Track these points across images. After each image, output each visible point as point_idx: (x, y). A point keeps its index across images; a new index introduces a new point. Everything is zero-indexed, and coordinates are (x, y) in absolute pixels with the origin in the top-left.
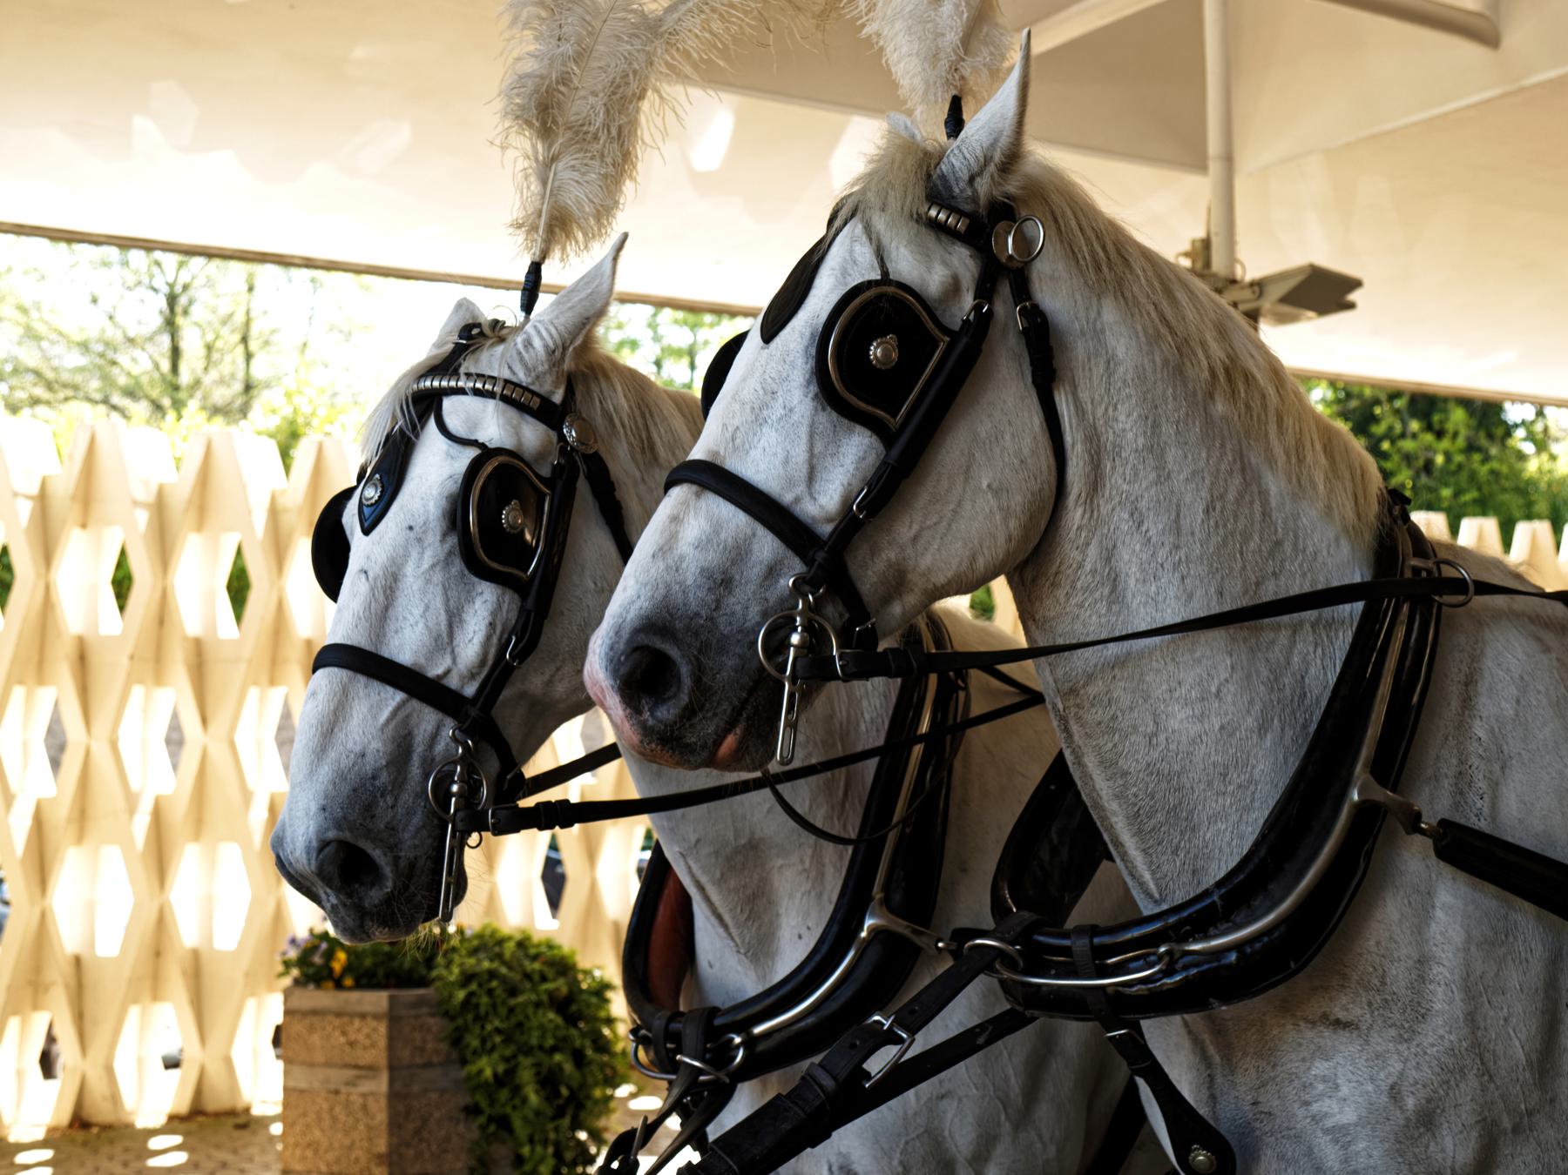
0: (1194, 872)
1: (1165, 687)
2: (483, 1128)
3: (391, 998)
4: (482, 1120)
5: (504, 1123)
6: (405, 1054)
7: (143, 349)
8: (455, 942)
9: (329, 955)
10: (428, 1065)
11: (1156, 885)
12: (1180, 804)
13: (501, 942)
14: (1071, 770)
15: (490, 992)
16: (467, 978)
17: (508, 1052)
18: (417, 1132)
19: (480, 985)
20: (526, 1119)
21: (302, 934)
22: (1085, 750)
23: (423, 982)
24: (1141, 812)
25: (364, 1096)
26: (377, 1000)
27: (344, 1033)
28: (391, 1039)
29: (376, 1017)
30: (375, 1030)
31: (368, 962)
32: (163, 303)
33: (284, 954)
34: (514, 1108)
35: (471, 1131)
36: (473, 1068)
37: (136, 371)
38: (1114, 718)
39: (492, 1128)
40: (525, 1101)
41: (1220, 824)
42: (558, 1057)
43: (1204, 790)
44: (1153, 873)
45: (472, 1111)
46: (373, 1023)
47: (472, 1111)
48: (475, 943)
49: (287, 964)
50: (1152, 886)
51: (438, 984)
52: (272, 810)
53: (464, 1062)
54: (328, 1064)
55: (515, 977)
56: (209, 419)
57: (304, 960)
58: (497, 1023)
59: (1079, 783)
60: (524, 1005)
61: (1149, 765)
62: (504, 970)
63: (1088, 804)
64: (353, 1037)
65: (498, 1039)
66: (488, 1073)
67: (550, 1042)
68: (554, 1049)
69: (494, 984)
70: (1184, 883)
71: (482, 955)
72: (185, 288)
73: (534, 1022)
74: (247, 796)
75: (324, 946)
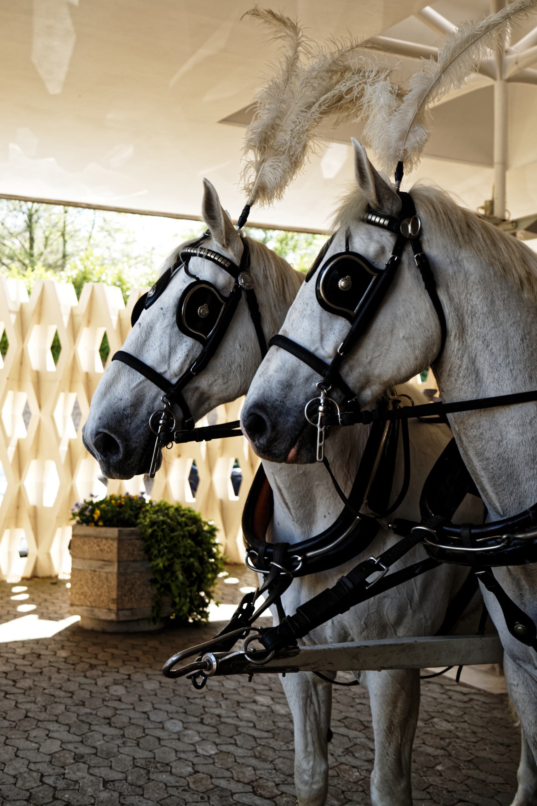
0: (519, 503)
1: (505, 419)
2: (158, 589)
3: (120, 532)
4: (158, 586)
5: (168, 588)
6: (125, 556)
7: (17, 238)
8: (148, 508)
9: (93, 512)
10: (135, 561)
11: (502, 508)
12: (513, 472)
13: (168, 508)
14: (462, 457)
15: (163, 530)
16: (153, 523)
17: (170, 557)
18: (130, 590)
19: (158, 527)
20: (177, 586)
21: (81, 502)
22: (469, 448)
23: (134, 525)
24: (495, 476)
25: (107, 573)
26: (113, 532)
27: (98, 546)
28: (119, 549)
29: (112, 539)
30: (112, 545)
31: (110, 515)
32: (26, 217)
33: (73, 510)
34: (172, 581)
35: (154, 590)
36: (155, 563)
37: (14, 248)
38: (482, 434)
39: (162, 590)
40: (177, 578)
41: (531, 482)
42: (192, 560)
43: (524, 467)
44: (500, 503)
45: (154, 581)
46: (111, 542)
47: (154, 581)
48: (157, 508)
49: (74, 515)
50: (500, 509)
51: (140, 526)
52: (70, 446)
53: (150, 560)
54: (91, 559)
55: (174, 524)
56: (47, 270)
57: (81, 513)
58: (165, 544)
59: (466, 463)
60: (178, 536)
61: (498, 455)
62: (169, 521)
63: (470, 473)
64: (102, 548)
65: (165, 551)
66: (161, 565)
67: (189, 553)
68: (190, 556)
69: (165, 526)
70: (515, 508)
71: (159, 514)
72: (36, 211)
73: (182, 544)
74: (59, 440)
75: (90, 507)
